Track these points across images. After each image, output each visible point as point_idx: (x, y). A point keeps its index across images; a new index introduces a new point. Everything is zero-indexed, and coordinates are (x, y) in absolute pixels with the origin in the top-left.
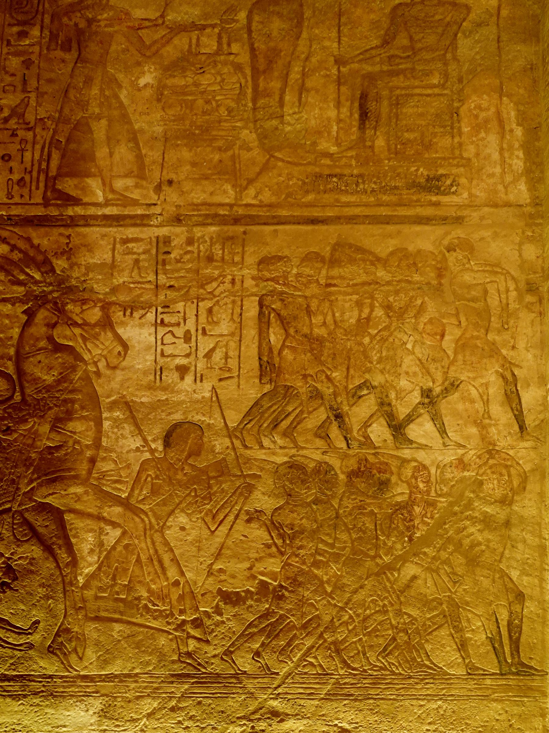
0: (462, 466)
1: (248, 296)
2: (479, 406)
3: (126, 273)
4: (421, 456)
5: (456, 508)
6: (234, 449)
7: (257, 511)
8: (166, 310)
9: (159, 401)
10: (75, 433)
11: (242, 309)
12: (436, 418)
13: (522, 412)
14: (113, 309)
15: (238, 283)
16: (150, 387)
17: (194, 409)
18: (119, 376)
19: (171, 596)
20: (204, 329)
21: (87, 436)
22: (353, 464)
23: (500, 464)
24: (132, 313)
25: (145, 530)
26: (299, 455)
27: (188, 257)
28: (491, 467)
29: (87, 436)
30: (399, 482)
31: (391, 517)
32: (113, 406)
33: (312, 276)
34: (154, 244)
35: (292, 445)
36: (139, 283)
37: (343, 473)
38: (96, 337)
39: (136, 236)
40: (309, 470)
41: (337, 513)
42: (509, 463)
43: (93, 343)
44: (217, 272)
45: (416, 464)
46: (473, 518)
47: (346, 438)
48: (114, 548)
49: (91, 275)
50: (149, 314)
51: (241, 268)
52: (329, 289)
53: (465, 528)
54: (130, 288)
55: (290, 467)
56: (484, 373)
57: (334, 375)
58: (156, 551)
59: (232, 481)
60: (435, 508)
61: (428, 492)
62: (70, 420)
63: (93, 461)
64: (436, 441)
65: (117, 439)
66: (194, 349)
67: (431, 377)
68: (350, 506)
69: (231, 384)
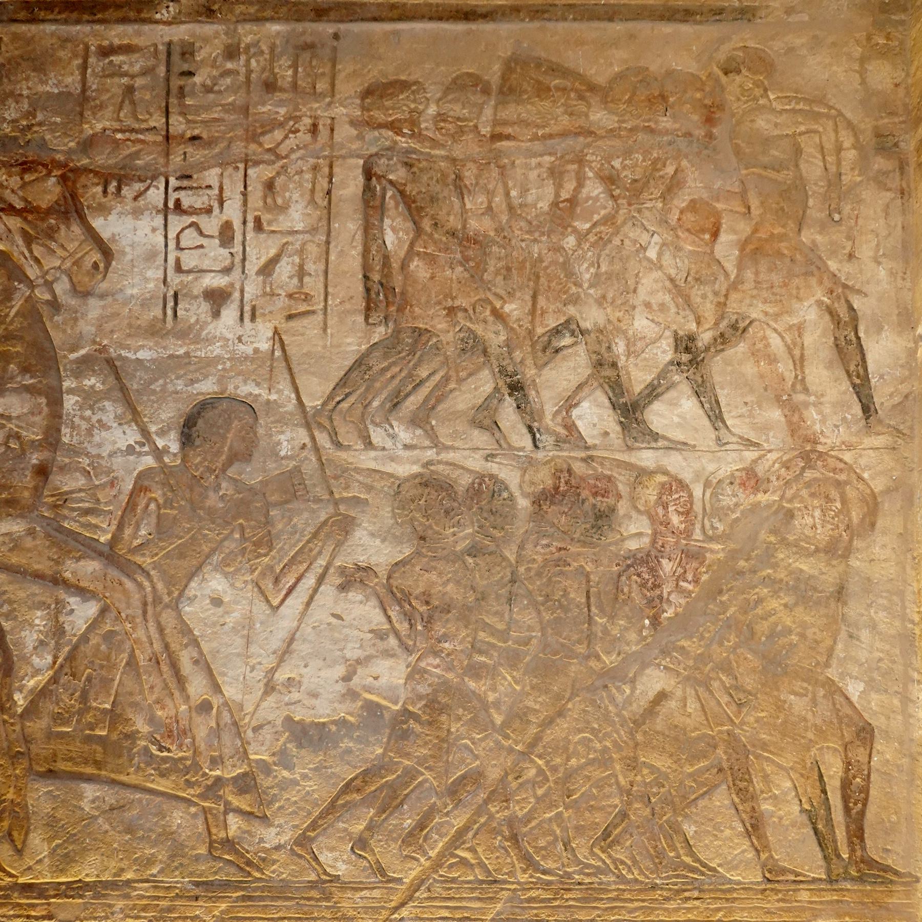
0: (753, 482)
1: (343, 157)
2: (785, 368)
3: (109, 112)
4: (675, 463)
6: (317, 449)
7: (359, 568)
8: (185, 183)
9: (171, 357)
11: (331, 182)
12: (702, 390)
13: (866, 378)
14: (83, 180)
15: (324, 132)
16: (155, 331)
17: (239, 374)
18: (94, 309)
19: (195, 731)
20: (258, 220)
21: (33, 425)
22: (544, 478)
24: (119, 189)
25: (145, 604)
26: (439, 462)
27: (228, 81)
28: (808, 485)
29: (33, 425)
30: (634, 514)
32: (84, 365)
33: (465, 120)
34: (163, 57)
35: (427, 443)
36: (133, 130)
37: (525, 495)
38: (51, 233)
39: (126, 42)
40: (461, 490)
42: (843, 477)
43: (42, 245)
44: (283, 111)
45: (664, 479)
47: (530, 429)
48: (85, 638)
49: (40, 117)
50: (152, 190)
51: (329, 104)
52: (498, 144)
54: (116, 142)
55: (426, 485)
56: (796, 305)
57: (508, 308)
58: (167, 647)
60: (702, 564)
61: (688, 533)
63: (43, 471)
64: (705, 435)
65: (90, 432)
66: (238, 258)
67: (694, 311)
68: (539, 558)
69: (310, 327)
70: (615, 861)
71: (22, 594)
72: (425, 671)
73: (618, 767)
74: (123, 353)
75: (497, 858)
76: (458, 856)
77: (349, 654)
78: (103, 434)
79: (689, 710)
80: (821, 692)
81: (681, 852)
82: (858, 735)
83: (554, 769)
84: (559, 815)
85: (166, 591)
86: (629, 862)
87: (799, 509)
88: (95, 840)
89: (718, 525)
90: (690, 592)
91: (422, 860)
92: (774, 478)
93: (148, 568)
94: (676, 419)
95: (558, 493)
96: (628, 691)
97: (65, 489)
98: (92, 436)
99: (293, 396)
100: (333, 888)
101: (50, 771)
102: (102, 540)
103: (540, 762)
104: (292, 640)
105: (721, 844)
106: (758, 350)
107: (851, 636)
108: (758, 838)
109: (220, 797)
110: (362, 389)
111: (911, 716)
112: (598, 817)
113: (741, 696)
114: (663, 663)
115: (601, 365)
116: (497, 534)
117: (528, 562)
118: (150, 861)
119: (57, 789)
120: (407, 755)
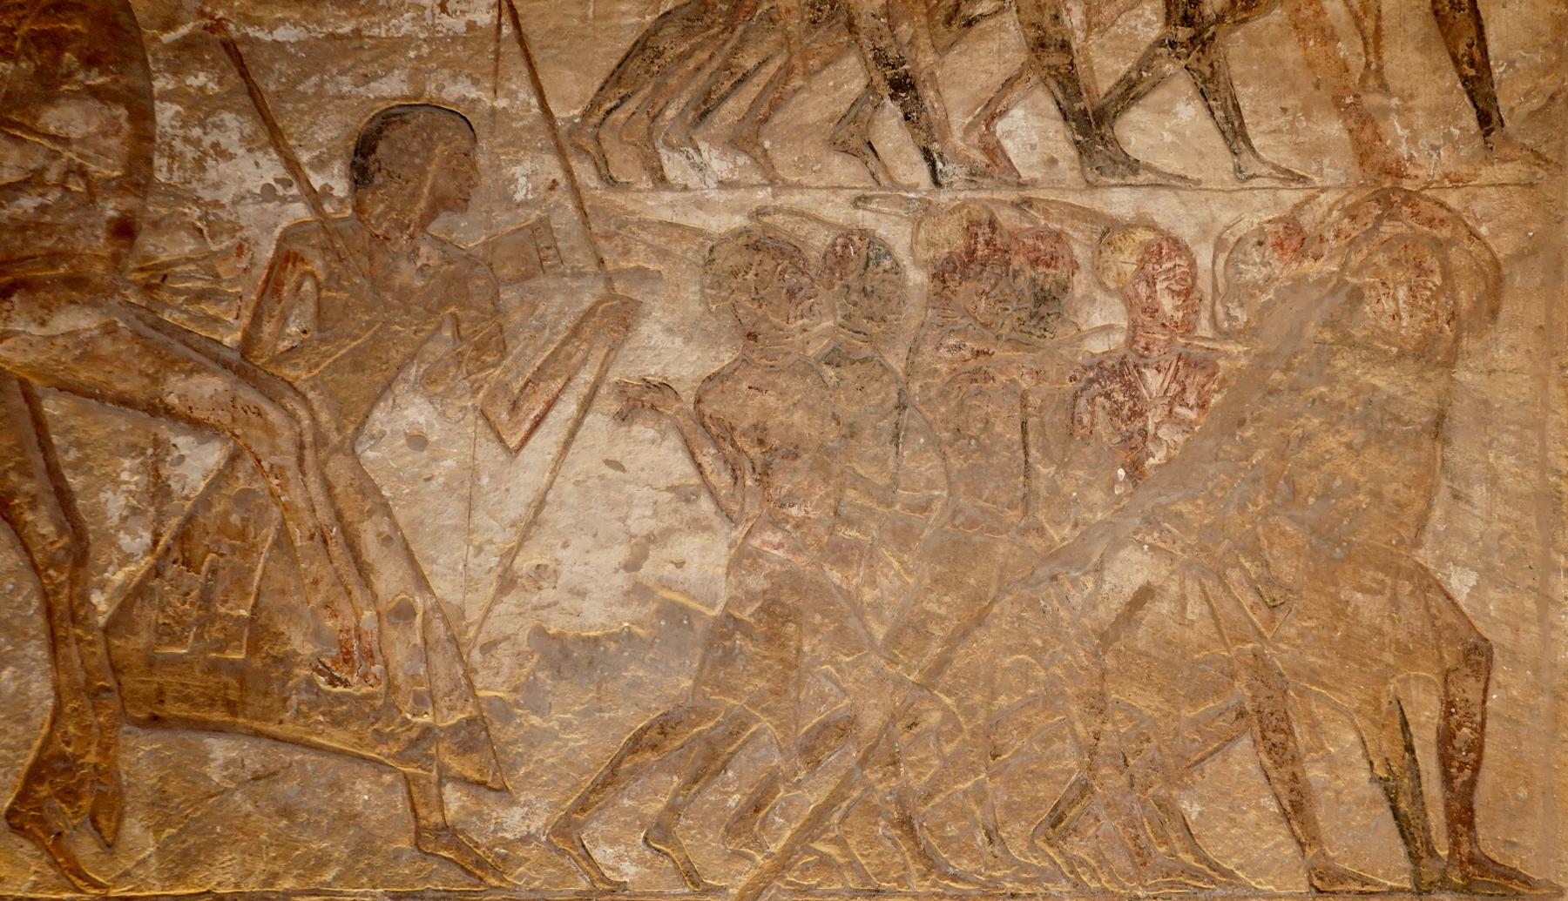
0: (1295, 241)
4: (1166, 210)
6: (575, 190)
7: (648, 385)
9: (332, 37)
10: (66, 141)
12: (1212, 88)
17: (444, 65)
21: (103, 153)
22: (950, 235)
26: (777, 210)
28: (1386, 245)
30: (1099, 295)
35: (757, 178)
37: (917, 263)
40: (814, 256)
42: (1444, 233)
45: (1150, 236)
47: (927, 154)
48: (205, 501)
53: (1306, 438)
58: (339, 516)
61: (1188, 327)
62: (50, 99)
63: (124, 230)
64: (1217, 163)
65: (200, 165)
68: (943, 368)
71: (98, 433)
73: (1075, 709)
74: (252, 32)
75: (880, 855)
76: (816, 852)
77: (634, 526)
78: (223, 166)
79: (1190, 616)
80: (1407, 587)
81: (1178, 845)
82: (1466, 657)
84: (979, 786)
85: (333, 425)
86: (1093, 863)
87: (1372, 287)
88: (230, 827)
89: (1237, 312)
90: (1191, 424)
91: (759, 858)
92: (1330, 235)
93: (303, 387)
94: (1168, 137)
95: (974, 260)
96: (1090, 585)
97: (164, 258)
98: (203, 169)
99: (534, 101)
101: (155, 718)
102: (227, 341)
104: (541, 503)
106: (1305, 21)
107: (1456, 497)
109: (431, 758)
110: (648, 90)
111: (1553, 627)
115: (1043, 46)
116: (873, 328)
117: (926, 375)
118: (322, 862)
119: (170, 748)
120: (732, 690)
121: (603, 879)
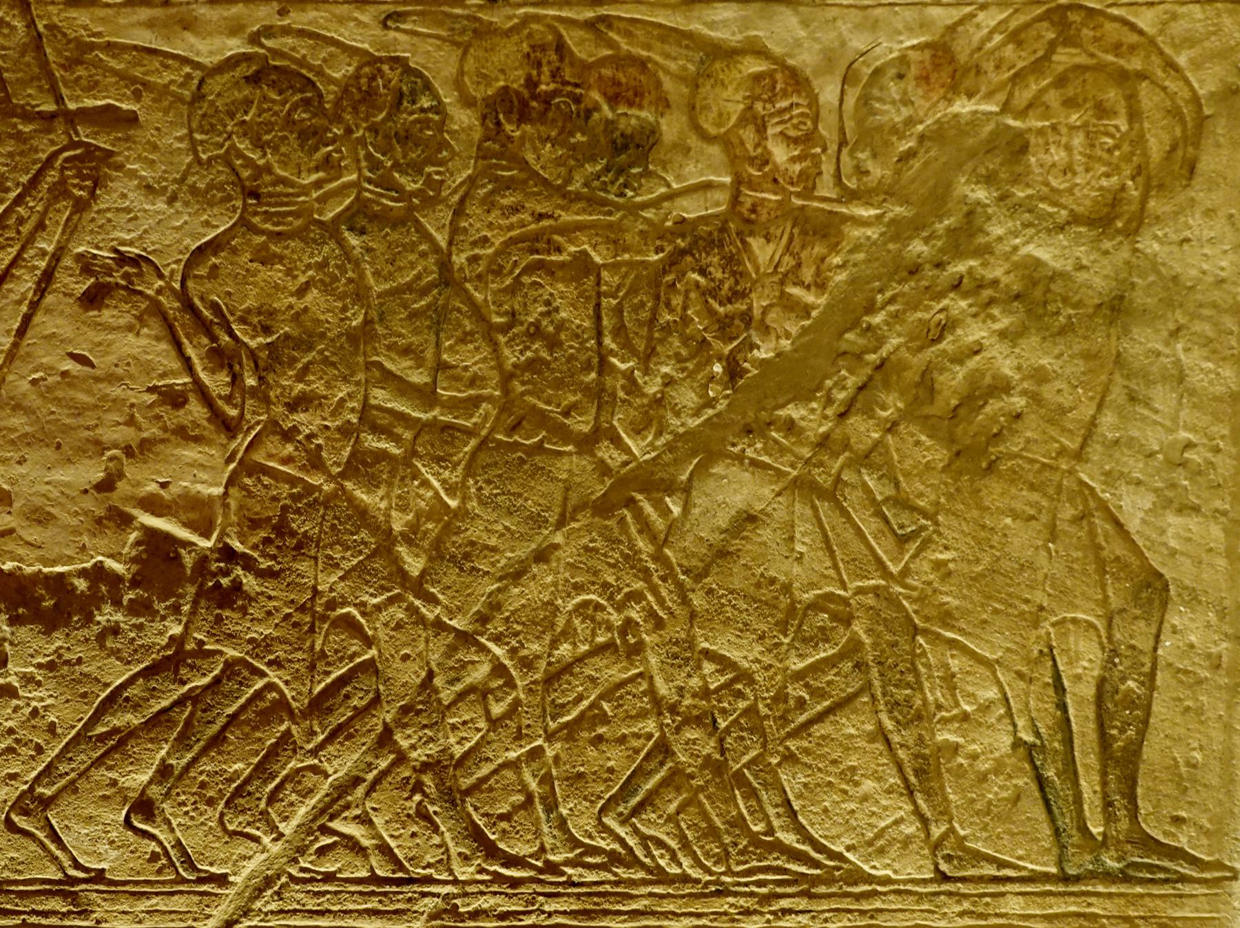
5: (918, 247)
7: (122, 259)
22: (506, 67)
23: (1100, 68)
26: (286, 31)
28: (1061, 82)
30: (693, 141)
31: (657, 284)
37: (467, 102)
40: (330, 93)
41: (445, 265)
42: (1135, 64)
46: (980, 285)
53: (946, 328)
55: (254, 80)
59: (19, 137)
60: (834, 248)
61: (808, 182)
70: (644, 840)
72: (266, 471)
73: (653, 661)
75: (414, 835)
76: (334, 833)
79: (799, 548)
80: (1068, 512)
82: (1136, 597)
83: (527, 664)
87: (1041, 132)
89: (870, 165)
90: (806, 310)
91: (266, 840)
92: (989, 66)
96: (676, 510)
100: (91, 893)
103: (498, 651)
105: (854, 807)
107: (1133, 398)
108: (929, 794)
112: (615, 757)
113: (905, 518)
114: (750, 453)
116: (411, 185)
117: (474, 244)
121: (77, 865)
